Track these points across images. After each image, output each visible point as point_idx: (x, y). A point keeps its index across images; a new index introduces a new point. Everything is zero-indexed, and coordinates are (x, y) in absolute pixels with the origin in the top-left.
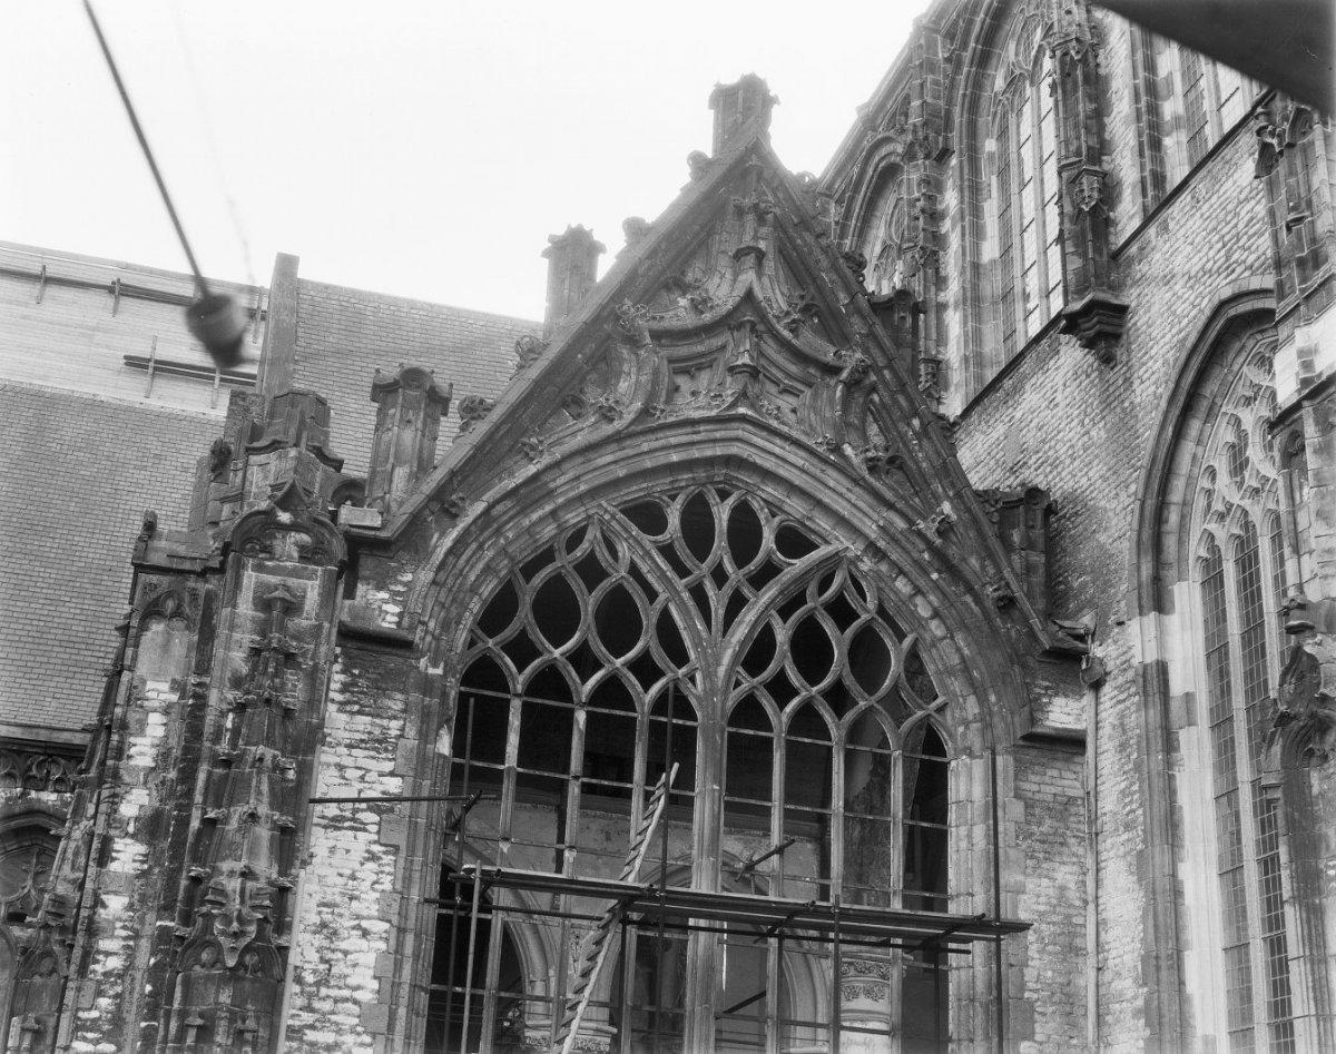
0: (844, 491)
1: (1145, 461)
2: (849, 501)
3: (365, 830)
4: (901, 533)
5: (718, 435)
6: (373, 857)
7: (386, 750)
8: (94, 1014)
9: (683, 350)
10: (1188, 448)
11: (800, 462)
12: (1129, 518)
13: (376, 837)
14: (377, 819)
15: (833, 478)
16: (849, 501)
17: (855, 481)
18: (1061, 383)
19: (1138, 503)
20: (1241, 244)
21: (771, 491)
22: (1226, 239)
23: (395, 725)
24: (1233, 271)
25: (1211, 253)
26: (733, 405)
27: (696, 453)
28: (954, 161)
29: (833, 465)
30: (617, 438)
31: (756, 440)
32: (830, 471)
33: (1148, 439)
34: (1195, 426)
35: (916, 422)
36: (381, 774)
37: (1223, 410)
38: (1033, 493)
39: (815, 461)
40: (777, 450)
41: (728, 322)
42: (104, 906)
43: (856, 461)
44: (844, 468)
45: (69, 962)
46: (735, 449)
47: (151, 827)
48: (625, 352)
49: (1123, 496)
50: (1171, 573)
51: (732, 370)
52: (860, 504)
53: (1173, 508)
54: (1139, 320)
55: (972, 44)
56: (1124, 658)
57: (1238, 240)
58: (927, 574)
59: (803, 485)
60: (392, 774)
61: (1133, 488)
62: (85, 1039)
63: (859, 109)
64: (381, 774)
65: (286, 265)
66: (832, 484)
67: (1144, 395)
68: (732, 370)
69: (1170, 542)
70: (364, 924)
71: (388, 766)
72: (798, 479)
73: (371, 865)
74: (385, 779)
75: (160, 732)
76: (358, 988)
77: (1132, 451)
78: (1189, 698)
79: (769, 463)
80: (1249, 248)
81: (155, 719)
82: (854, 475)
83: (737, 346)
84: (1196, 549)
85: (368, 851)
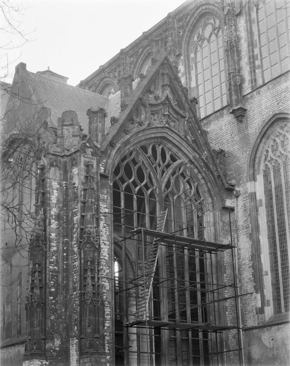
0: (186, 147)
1: (252, 147)
2: (187, 150)
3: (102, 221)
4: (198, 158)
5: (162, 131)
6: (105, 227)
7: (105, 202)
8: (53, 260)
9: (154, 109)
10: (262, 145)
11: (178, 139)
12: (247, 159)
13: (104, 222)
14: (104, 218)
15: (184, 144)
16: (187, 150)
17: (189, 145)
18: (224, 124)
19: (250, 156)
20: (282, 102)
21: (170, 145)
22: (278, 100)
23: (106, 196)
24: (279, 108)
25: (273, 102)
26: (165, 125)
27: (157, 135)
28: (182, 58)
29: (185, 141)
30: (143, 130)
31: (170, 134)
32: (184, 142)
33: (253, 142)
34: (264, 140)
35: (199, 132)
36: (104, 208)
37: (271, 137)
38: (222, 151)
39: (181, 139)
40: (173, 136)
41: (163, 104)
42: (51, 235)
43: (190, 140)
44: (187, 141)
45: (46, 248)
46: (164, 135)
47: (58, 217)
48: (142, 108)
49: (245, 154)
50: (256, 173)
51: (164, 115)
52: (190, 151)
53: (257, 158)
54: (250, 113)
55: (189, 26)
56: (245, 191)
57: (281, 101)
58: (203, 169)
59: (178, 145)
60: (106, 208)
61: (248, 152)
62: (51, 266)
63: (144, 33)
64: (104, 208)
65: (21, 68)
66: (184, 145)
67: (252, 131)
68: (164, 115)
69: (256, 166)
70: (105, 242)
71: (105, 206)
72: (177, 144)
73: (104, 229)
74: (105, 209)
75: (57, 195)
76: (105, 256)
77: (248, 144)
78: (261, 200)
79: (171, 139)
80: (284, 103)
81: (55, 191)
82: (189, 144)
83: (164, 109)
84: (262, 167)
85: (104, 225)
